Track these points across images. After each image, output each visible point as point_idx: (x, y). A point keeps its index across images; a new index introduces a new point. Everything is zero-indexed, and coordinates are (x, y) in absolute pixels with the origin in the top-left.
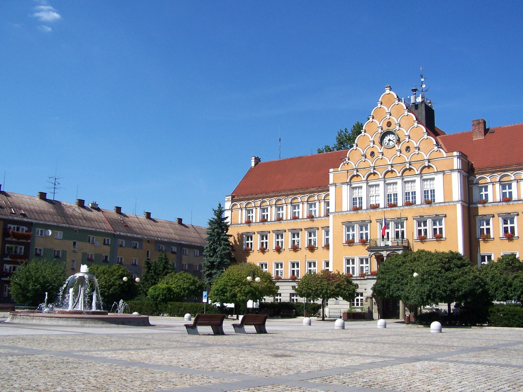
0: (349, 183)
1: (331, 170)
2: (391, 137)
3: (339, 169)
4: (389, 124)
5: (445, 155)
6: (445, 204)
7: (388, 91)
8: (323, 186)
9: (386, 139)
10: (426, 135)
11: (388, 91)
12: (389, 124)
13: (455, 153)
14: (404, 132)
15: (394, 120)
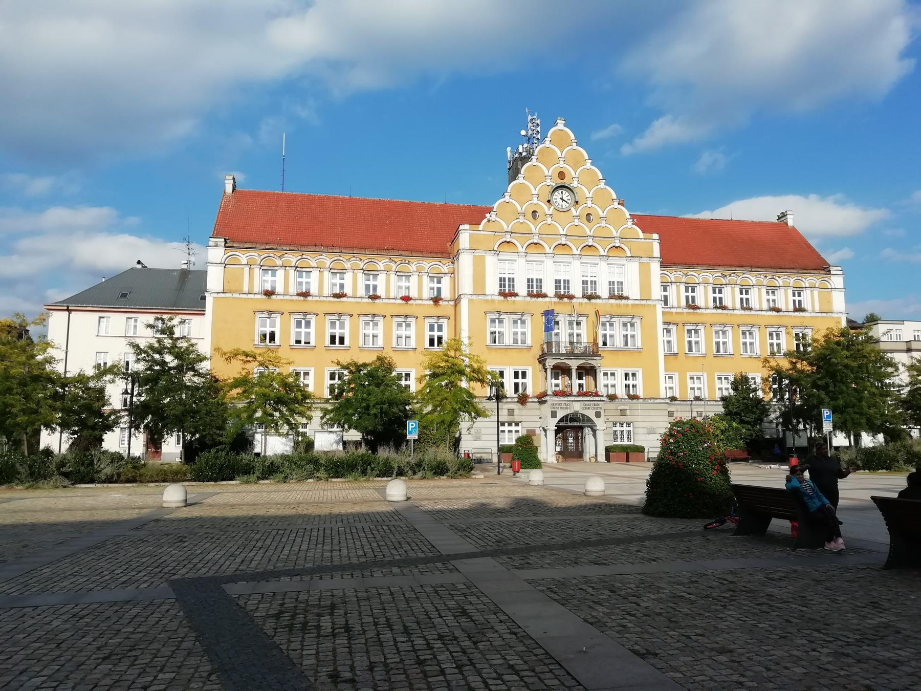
0: (497, 253)
1: (467, 227)
2: (566, 195)
3: (481, 227)
4: (562, 175)
5: (641, 235)
6: (643, 302)
7: (561, 125)
8: (446, 250)
9: (557, 195)
10: (616, 203)
11: (561, 125)
12: (562, 175)
13: (656, 236)
14: (585, 192)
15: (570, 171)
